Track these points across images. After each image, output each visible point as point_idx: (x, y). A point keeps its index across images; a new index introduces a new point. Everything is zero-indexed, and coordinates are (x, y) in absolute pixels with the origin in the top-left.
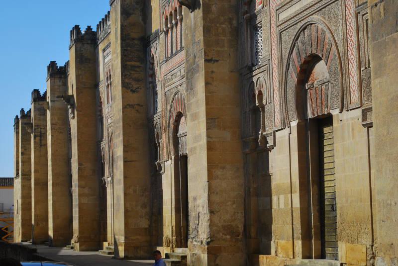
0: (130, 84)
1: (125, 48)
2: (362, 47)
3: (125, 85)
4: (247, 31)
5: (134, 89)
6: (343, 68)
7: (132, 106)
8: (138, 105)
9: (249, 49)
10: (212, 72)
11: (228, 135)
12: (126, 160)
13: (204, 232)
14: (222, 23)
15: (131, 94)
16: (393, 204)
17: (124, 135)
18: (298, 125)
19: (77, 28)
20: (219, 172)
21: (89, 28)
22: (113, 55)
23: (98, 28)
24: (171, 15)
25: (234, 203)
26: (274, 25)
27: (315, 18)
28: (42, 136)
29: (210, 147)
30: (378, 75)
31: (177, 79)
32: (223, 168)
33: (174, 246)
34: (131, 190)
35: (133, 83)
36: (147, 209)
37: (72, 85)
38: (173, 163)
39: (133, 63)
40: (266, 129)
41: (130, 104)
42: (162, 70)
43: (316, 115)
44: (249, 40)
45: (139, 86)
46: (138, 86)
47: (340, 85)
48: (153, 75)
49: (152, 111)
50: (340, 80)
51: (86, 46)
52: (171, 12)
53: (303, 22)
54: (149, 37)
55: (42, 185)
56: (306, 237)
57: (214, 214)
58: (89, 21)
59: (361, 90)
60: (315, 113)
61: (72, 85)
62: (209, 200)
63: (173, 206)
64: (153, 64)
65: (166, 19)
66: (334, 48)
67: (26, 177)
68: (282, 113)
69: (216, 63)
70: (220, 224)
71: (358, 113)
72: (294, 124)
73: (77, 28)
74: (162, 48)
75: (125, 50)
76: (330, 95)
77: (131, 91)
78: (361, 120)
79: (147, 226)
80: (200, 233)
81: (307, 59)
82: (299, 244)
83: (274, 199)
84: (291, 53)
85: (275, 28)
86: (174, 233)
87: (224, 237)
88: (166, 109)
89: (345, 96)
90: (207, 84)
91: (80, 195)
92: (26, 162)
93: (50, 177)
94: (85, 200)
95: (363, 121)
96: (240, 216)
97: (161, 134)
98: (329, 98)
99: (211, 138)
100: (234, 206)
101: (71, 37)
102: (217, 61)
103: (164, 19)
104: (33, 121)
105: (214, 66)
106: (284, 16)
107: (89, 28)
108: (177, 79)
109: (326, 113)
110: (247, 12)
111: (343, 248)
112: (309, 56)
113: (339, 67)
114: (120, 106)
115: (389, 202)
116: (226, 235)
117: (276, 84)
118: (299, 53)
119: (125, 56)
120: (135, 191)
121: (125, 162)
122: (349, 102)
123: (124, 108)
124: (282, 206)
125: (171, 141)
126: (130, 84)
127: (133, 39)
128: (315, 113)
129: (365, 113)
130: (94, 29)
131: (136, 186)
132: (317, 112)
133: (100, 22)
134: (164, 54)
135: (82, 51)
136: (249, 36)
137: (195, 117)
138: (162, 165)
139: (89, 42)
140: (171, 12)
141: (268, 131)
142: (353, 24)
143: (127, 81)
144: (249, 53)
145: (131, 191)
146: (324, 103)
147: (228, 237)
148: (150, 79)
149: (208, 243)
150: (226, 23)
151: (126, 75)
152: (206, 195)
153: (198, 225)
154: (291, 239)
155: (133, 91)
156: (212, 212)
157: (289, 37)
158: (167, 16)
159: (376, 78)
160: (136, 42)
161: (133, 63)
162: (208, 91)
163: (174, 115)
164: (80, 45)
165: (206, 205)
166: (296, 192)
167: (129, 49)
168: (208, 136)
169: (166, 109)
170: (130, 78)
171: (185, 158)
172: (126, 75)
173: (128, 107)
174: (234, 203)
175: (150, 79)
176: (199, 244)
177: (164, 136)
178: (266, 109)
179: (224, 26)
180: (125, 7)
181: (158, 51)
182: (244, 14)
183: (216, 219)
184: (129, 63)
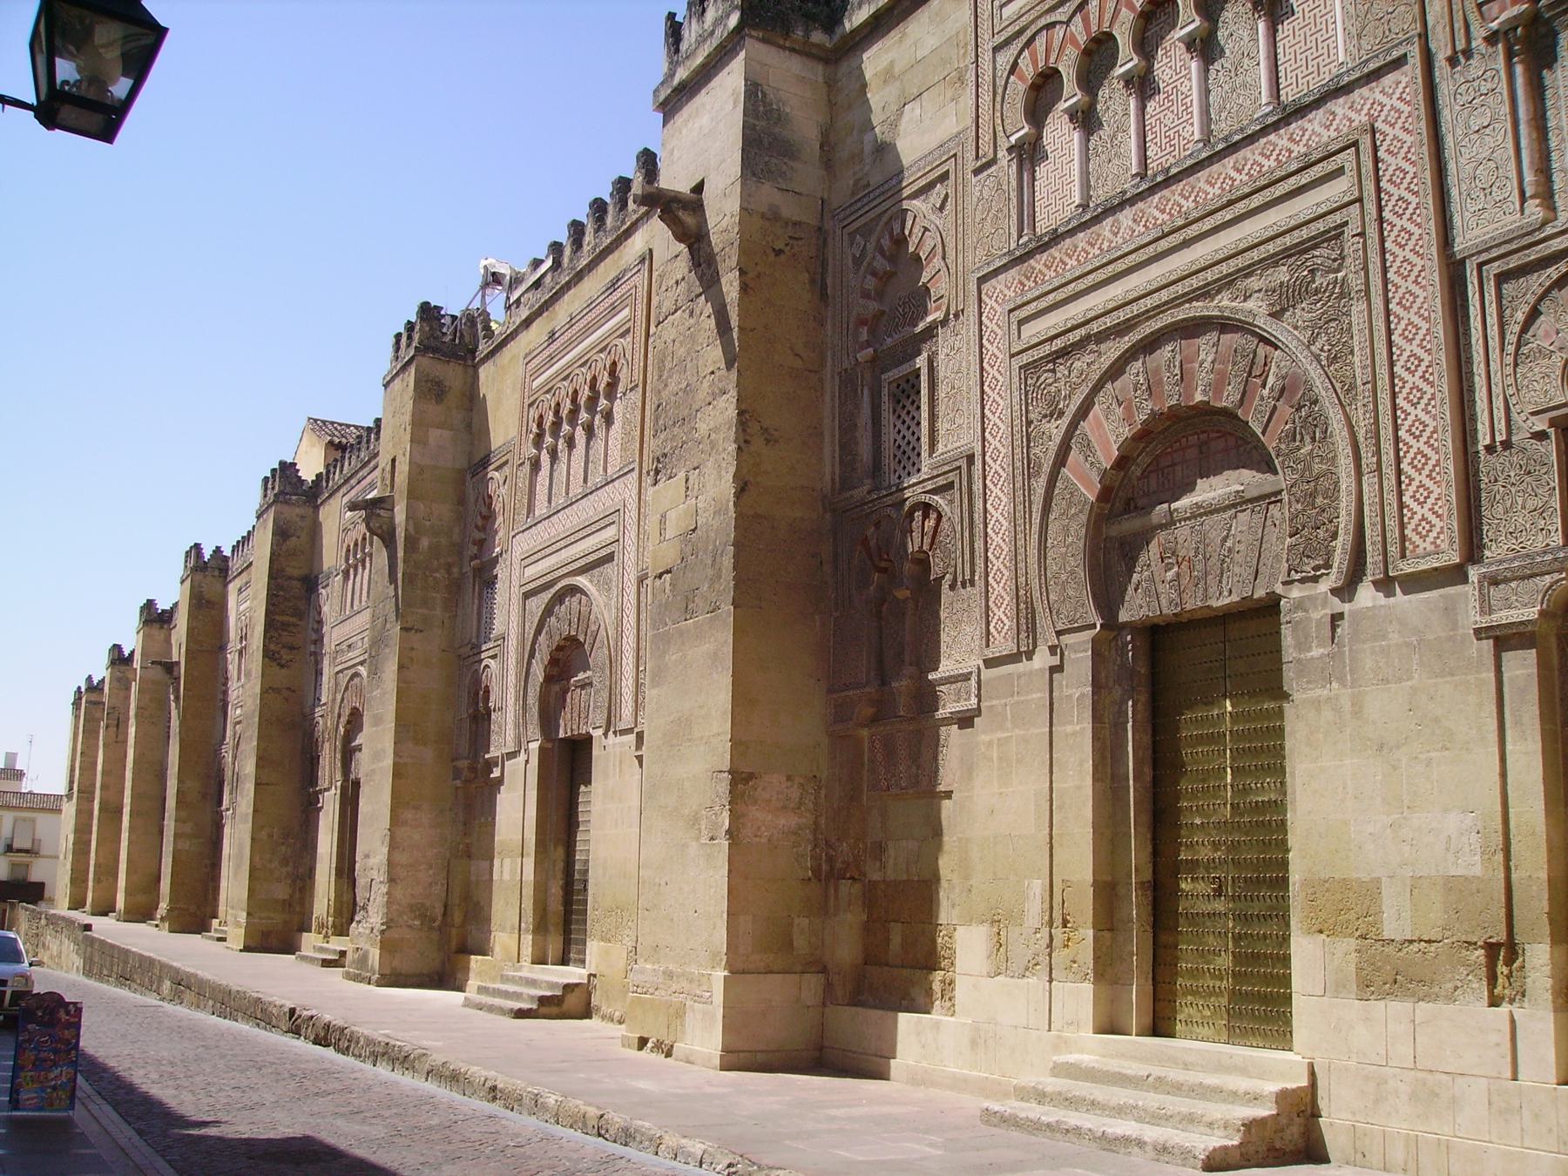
0: (278, 653)
2: (642, 633)
3: (268, 654)
4: (474, 585)
5: (283, 662)
6: (614, 664)
7: (277, 691)
8: (289, 689)
9: (475, 616)
10: (413, 649)
11: (429, 754)
12: (259, 781)
13: (377, 913)
14: (437, 571)
16: (663, 883)
17: (259, 738)
18: (540, 748)
19: (197, 547)
20: (408, 815)
21: (218, 550)
22: (252, 602)
23: (233, 551)
24: (356, 544)
25: (431, 868)
26: (516, 583)
27: (582, 581)
28: (119, 724)
29: (398, 773)
30: (656, 683)
31: (357, 652)
32: (416, 808)
33: (330, 932)
34: (263, 833)
36: (289, 869)
38: (339, 791)
39: (286, 618)
40: (492, 749)
41: (275, 686)
42: (333, 637)
43: (569, 734)
44: (476, 601)
46: (289, 657)
47: (607, 690)
48: (319, 641)
49: (310, 701)
50: (608, 683)
51: (209, 579)
52: (357, 540)
53: (557, 587)
54: (317, 577)
55: (112, 812)
56: (540, 928)
57: (396, 883)
58: (220, 536)
59: (636, 701)
60: (569, 730)
62: (388, 860)
63: (334, 865)
64: (320, 622)
65: (348, 550)
66: (602, 632)
67: (86, 794)
68: (517, 726)
69: (419, 634)
71: (632, 738)
72: (534, 746)
73: (197, 547)
74: (336, 601)
76: (592, 703)
77: (278, 664)
78: (633, 748)
79: (287, 897)
80: (370, 913)
81: (562, 643)
82: (528, 939)
83: (496, 862)
84: (538, 632)
85: (517, 587)
86: (332, 911)
87: (411, 922)
88: (334, 700)
89: (613, 708)
90: (401, 667)
91: (176, 836)
92: (88, 766)
93: (127, 800)
94: (185, 845)
95: (636, 750)
96: (439, 890)
97: (323, 742)
98: (591, 708)
99: (401, 757)
100: (431, 872)
101: (186, 561)
102: (421, 631)
103: (344, 550)
104: (106, 699)
105: (415, 638)
106: (532, 571)
107: (218, 550)
108: (357, 652)
109: (584, 732)
110: (475, 557)
111: (593, 948)
112: (564, 639)
113: (608, 662)
114: (258, 689)
115: (657, 880)
116: (413, 920)
117: (512, 679)
118: (549, 633)
120: (270, 836)
121: (257, 784)
122: (618, 719)
123: (264, 691)
124: (506, 877)
125: (339, 756)
126: (278, 653)
127: (290, 578)
128: (569, 730)
129: (640, 736)
130: (227, 552)
132: (572, 730)
133: (238, 542)
134: (338, 609)
136: (476, 594)
137: (378, 720)
138: (320, 796)
139: (216, 573)
140: (357, 540)
141: (494, 752)
142: (633, 597)
143: (272, 647)
144: (475, 623)
145: (264, 834)
146: (583, 714)
147: (417, 922)
148: (312, 648)
149: (382, 932)
150: (442, 571)
152: (385, 850)
153: (369, 900)
154: (517, 931)
156: (392, 880)
157: (538, 604)
158: (349, 546)
159: (653, 687)
161: (286, 618)
162: (402, 680)
163: (347, 712)
164: (199, 576)
165: (384, 868)
166: (528, 855)
167: (281, 593)
168: (396, 754)
169: (334, 700)
171: (357, 784)
175: (312, 648)
176: (368, 931)
177: (327, 745)
178: (493, 717)
179: (438, 575)
181: (329, 602)
183: (399, 893)
184: (277, 617)
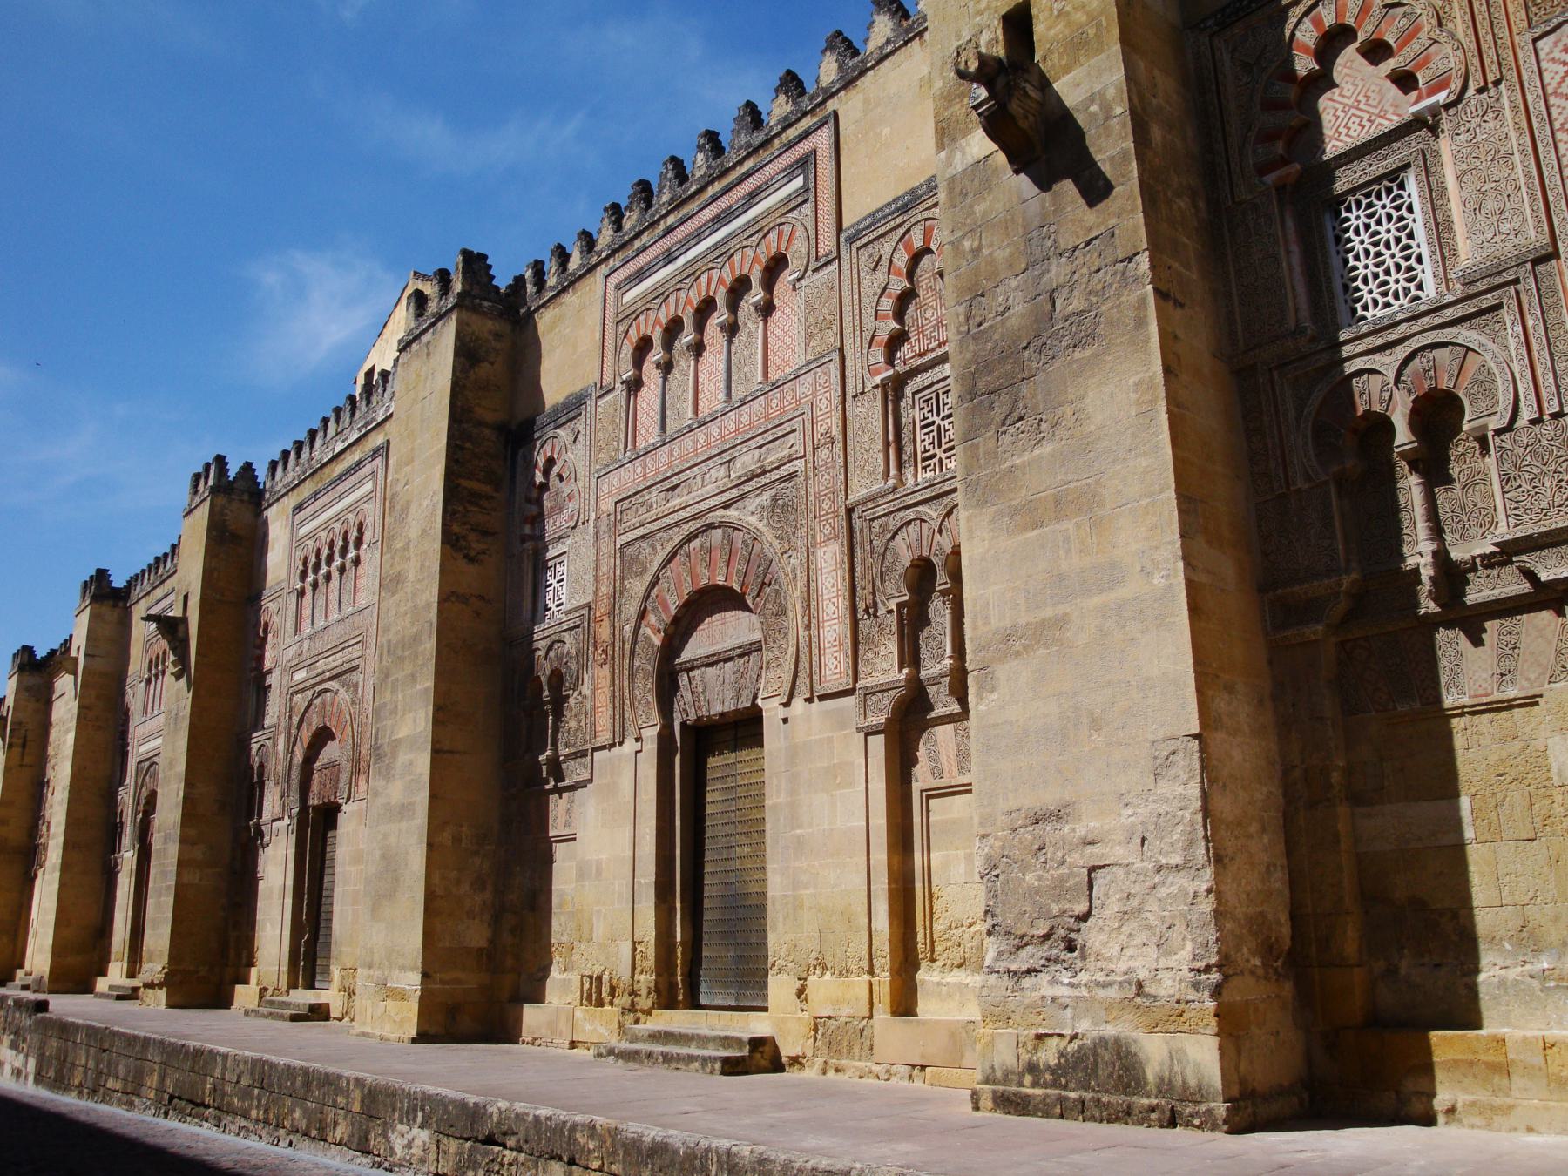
0: (464, 537)
1: (458, 443)
5: (473, 553)
7: (463, 599)
12: (438, 746)
15: (462, 563)
21: (248, 468)
34: (445, 834)
35: (472, 537)
37: (186, 597)
45: (485, 547)
46: (481, 547)
49: (526, 614)
61: (186, 597)
70: (1240, 912)
73: (221, 461)
75: (457, 445)
77: (466, 556)
79: (483, 943)
107: (248, 468)
119: (457, 461)
120: (457, 839)
127: (481, 423)
131: (461, 826)
135: (226, 515)
139: (246, 497)
143: (456, 528)
145: (446, 838)
148: (527, 530)
151: (454, 513)
155: (471, 560)
160: (487, 432)
167: (468, 445)
170: (465, 523)
172: (454, 513)
173: (453, 599)
174: (1263, 830)
175: (527, 530)
180: (467, 339)
182: (1262, 170)
184: (465, 483)
